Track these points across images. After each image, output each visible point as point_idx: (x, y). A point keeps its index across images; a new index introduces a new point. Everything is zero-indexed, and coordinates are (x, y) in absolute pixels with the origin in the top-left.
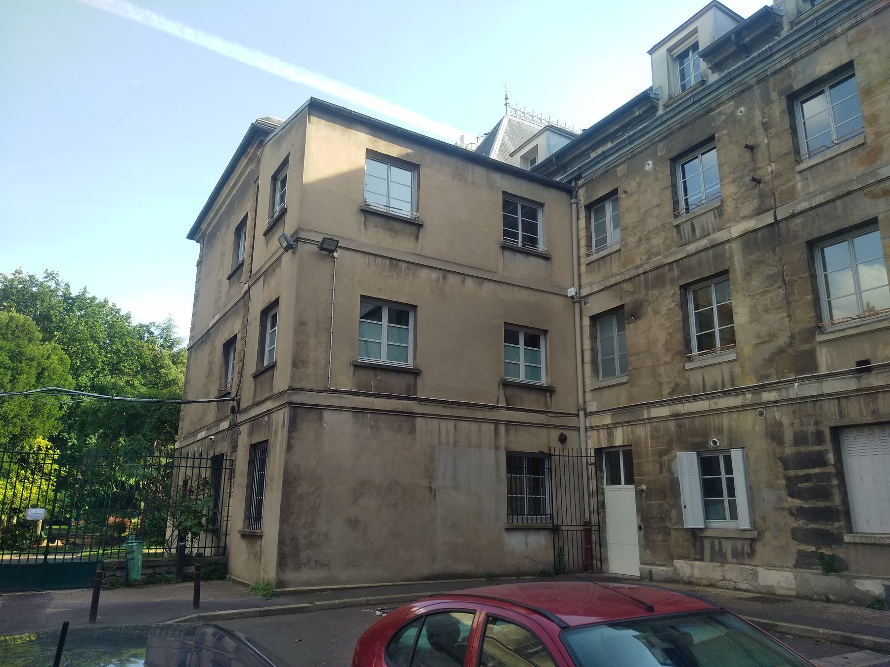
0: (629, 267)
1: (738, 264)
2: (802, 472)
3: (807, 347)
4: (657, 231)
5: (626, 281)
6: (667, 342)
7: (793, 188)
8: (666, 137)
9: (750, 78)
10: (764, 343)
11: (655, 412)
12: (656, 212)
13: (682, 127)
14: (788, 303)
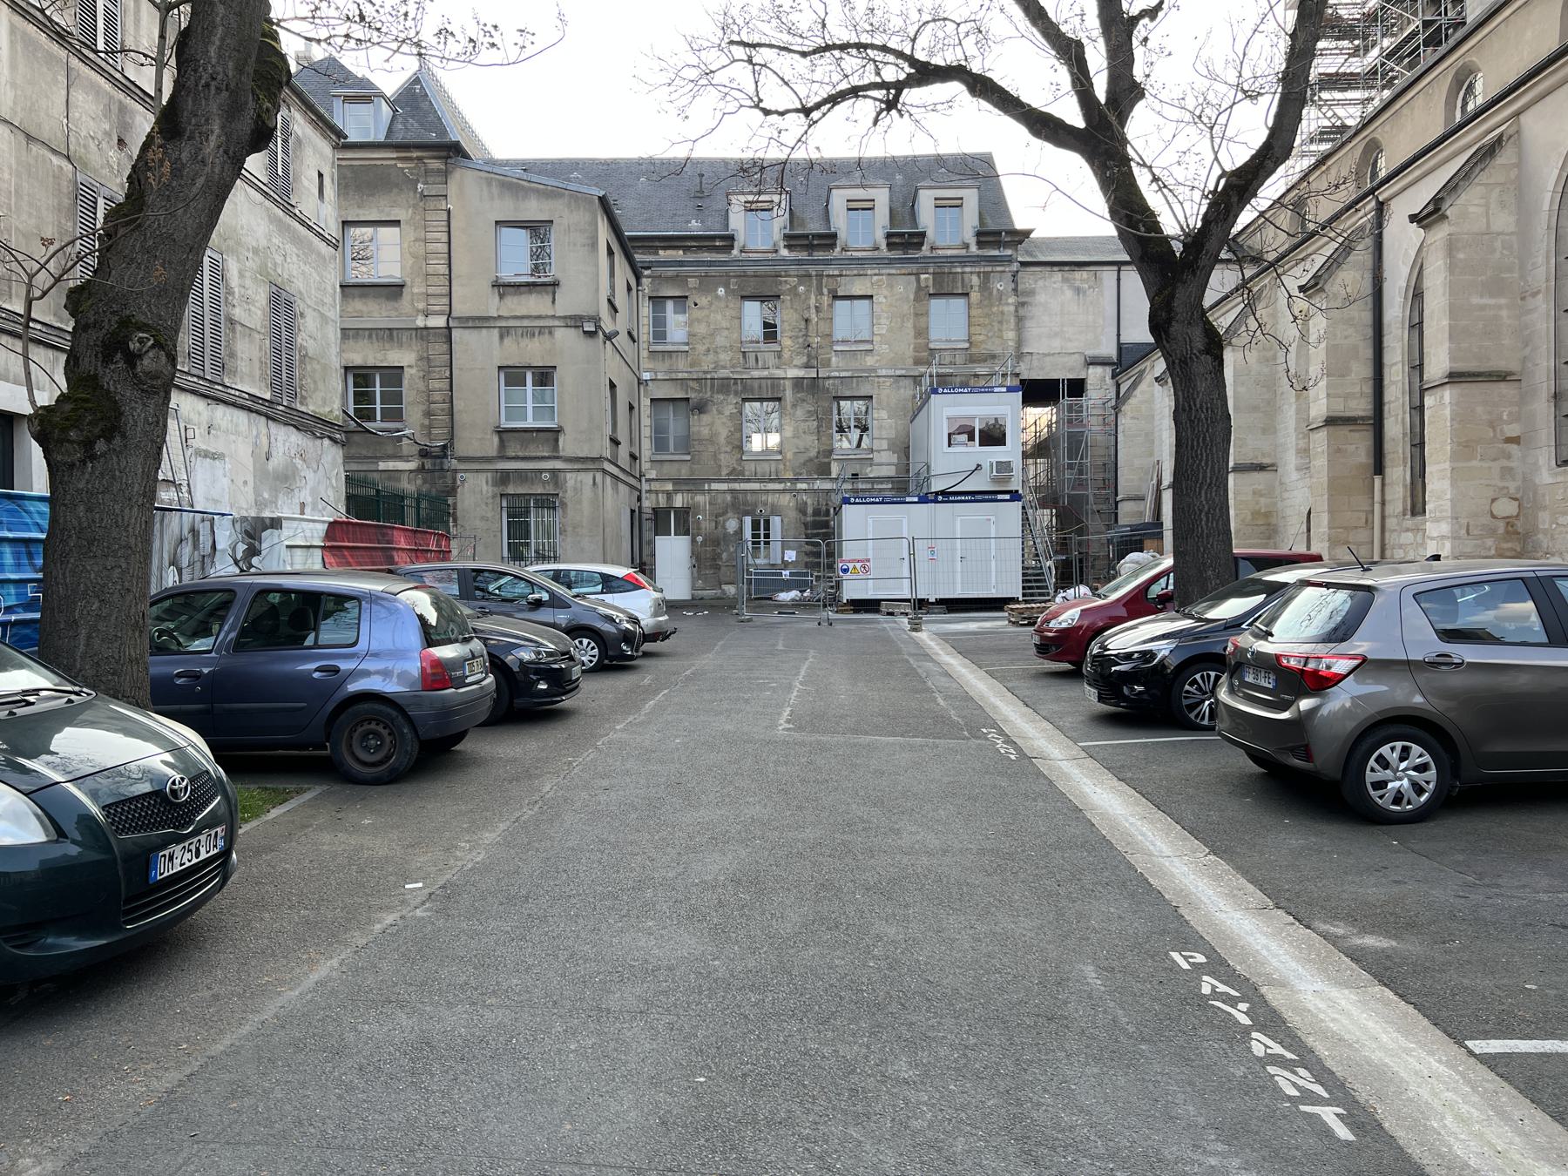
0: (697, 369)
1: (789, 395)
2: (815, 531)
3: (826, 460)
7: (830, 359)
9: (813, 270)
11: (715, 486)
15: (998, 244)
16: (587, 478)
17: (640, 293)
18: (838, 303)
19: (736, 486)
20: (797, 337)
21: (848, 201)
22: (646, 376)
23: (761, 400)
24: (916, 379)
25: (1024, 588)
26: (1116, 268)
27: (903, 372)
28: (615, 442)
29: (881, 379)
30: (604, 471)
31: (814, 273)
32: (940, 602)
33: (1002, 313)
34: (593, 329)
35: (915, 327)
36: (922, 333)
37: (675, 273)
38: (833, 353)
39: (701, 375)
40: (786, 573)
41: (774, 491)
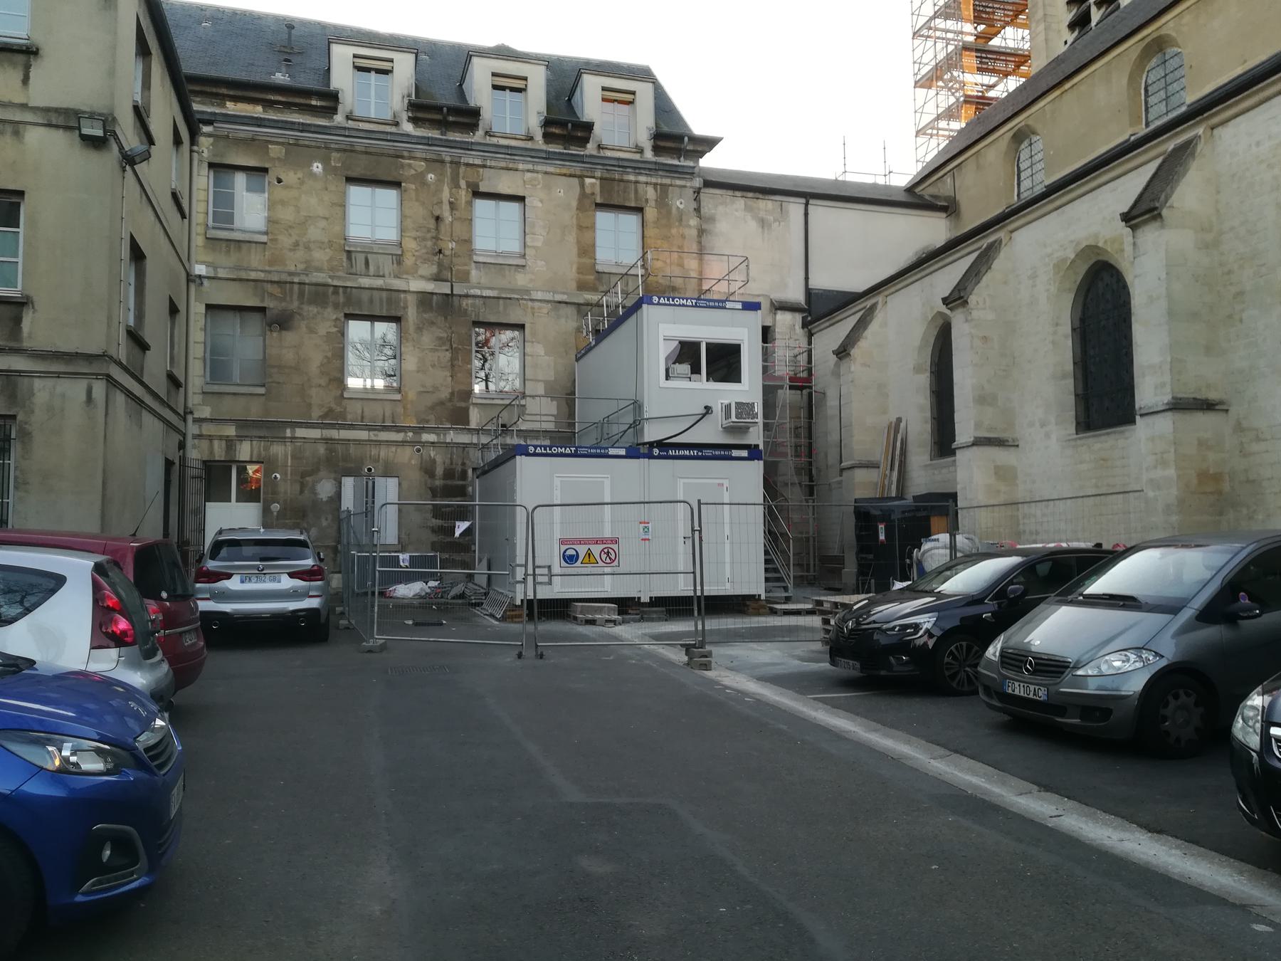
1: (412, 314)
3: (463, 404)
4: (321, 245)
5: (272, 282)
6: (322, 365)
7: (468, 273)
8: (345, 150)
9: (447, 154)
10: (428, 392)
11: (300, 433)
12: (323, 224)
13: (366, 153)
14: (453, 366)
15: (678, 152)
16: (76, 389)
17: (195, 155)
18: (480, 204)
19: (334, 434)
20: (424, 239)
21: (494, 75)
22: (200, 269)
23: (373, 318)
24: (582, 308)
25: (767, 580)
26: (803, 201)
27: (564, 298)
28: (137, 340)
29: (537, 304)
30: (109, 378)
31: (448, 159)
32: (657, 602)
33: (683, 236)
34: (100, 133)
35: (578, 242)
36: (587, 250)
37: (250, 135)
38: (473, 265)
39: (285, 277)
40: (404, 558)
41: (389, 443)
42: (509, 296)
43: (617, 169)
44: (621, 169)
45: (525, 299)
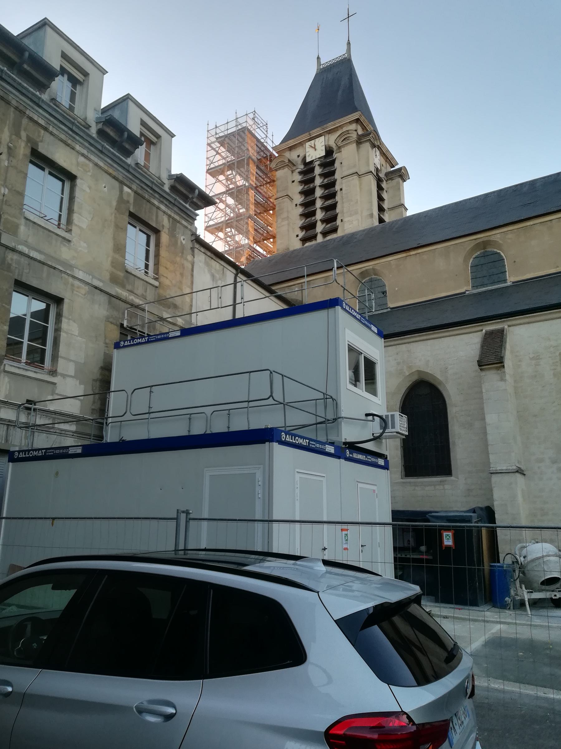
7: (17, 227)
15: (186, 198)
29: (77, 283)
38: (23, 221)
42: (54, 265)
43: (149, 190)
44: (151, 192)
45: (68, 274)
